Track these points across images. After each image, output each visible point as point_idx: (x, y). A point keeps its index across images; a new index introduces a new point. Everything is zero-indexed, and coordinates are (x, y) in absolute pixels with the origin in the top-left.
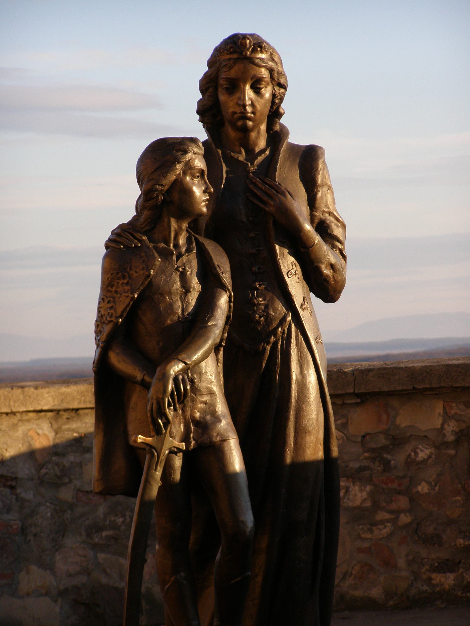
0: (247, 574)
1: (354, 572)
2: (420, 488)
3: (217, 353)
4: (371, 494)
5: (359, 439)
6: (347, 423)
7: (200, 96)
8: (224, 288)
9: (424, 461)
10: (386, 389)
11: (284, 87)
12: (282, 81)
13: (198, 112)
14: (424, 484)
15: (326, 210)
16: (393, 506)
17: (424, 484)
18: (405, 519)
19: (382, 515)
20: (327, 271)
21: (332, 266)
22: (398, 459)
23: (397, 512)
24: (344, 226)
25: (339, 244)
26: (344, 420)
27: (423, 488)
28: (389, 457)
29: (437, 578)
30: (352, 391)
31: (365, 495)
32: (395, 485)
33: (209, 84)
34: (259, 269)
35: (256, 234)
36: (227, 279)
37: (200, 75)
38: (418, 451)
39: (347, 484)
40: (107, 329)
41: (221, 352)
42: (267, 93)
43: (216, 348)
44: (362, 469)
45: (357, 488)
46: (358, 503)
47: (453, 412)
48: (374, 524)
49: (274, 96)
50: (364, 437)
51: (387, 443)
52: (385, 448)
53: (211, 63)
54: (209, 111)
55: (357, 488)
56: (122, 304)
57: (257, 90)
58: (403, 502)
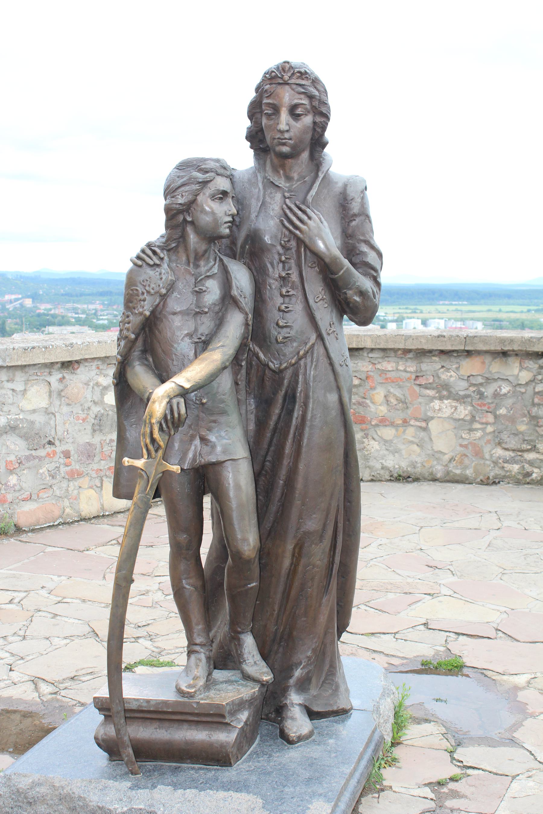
0: (252, 585)
1: (456, 459)
2: (501, 411)
3: (236, 374)
5: (466, 378)
9: (505, 395)
10: (484, 349)
11: (327, 117)
12: (324, 110)
13: (247, 138)
14: (504, 408)
15: (362, 238)
16: (484, 420)
17: (504, 408)
18: (490, 429)
19: (477, 426)
20: (357, 299)
21: (362, 293)
22: (489, 391)
23: (487, 424)
24: (380, 255)
26: (457, 365)
27: (502, 411)
29: (508, 466)
30: (462, 348)
31: (467, 412)
33: (255, 110)
35: (286, 258)
36: (247, 303)
38: (502, 388)
39: (457, 404)
40: (123, 343)
42: (308, 120)
45: (462, 407)
46: (462, 417)
47: (526, 366)
48: (471, 430)
50: (469, 377)
51: (484, 381)
52: (481, 384)
53: (257, 90)
55: (462, 407)
58: (490, 418)
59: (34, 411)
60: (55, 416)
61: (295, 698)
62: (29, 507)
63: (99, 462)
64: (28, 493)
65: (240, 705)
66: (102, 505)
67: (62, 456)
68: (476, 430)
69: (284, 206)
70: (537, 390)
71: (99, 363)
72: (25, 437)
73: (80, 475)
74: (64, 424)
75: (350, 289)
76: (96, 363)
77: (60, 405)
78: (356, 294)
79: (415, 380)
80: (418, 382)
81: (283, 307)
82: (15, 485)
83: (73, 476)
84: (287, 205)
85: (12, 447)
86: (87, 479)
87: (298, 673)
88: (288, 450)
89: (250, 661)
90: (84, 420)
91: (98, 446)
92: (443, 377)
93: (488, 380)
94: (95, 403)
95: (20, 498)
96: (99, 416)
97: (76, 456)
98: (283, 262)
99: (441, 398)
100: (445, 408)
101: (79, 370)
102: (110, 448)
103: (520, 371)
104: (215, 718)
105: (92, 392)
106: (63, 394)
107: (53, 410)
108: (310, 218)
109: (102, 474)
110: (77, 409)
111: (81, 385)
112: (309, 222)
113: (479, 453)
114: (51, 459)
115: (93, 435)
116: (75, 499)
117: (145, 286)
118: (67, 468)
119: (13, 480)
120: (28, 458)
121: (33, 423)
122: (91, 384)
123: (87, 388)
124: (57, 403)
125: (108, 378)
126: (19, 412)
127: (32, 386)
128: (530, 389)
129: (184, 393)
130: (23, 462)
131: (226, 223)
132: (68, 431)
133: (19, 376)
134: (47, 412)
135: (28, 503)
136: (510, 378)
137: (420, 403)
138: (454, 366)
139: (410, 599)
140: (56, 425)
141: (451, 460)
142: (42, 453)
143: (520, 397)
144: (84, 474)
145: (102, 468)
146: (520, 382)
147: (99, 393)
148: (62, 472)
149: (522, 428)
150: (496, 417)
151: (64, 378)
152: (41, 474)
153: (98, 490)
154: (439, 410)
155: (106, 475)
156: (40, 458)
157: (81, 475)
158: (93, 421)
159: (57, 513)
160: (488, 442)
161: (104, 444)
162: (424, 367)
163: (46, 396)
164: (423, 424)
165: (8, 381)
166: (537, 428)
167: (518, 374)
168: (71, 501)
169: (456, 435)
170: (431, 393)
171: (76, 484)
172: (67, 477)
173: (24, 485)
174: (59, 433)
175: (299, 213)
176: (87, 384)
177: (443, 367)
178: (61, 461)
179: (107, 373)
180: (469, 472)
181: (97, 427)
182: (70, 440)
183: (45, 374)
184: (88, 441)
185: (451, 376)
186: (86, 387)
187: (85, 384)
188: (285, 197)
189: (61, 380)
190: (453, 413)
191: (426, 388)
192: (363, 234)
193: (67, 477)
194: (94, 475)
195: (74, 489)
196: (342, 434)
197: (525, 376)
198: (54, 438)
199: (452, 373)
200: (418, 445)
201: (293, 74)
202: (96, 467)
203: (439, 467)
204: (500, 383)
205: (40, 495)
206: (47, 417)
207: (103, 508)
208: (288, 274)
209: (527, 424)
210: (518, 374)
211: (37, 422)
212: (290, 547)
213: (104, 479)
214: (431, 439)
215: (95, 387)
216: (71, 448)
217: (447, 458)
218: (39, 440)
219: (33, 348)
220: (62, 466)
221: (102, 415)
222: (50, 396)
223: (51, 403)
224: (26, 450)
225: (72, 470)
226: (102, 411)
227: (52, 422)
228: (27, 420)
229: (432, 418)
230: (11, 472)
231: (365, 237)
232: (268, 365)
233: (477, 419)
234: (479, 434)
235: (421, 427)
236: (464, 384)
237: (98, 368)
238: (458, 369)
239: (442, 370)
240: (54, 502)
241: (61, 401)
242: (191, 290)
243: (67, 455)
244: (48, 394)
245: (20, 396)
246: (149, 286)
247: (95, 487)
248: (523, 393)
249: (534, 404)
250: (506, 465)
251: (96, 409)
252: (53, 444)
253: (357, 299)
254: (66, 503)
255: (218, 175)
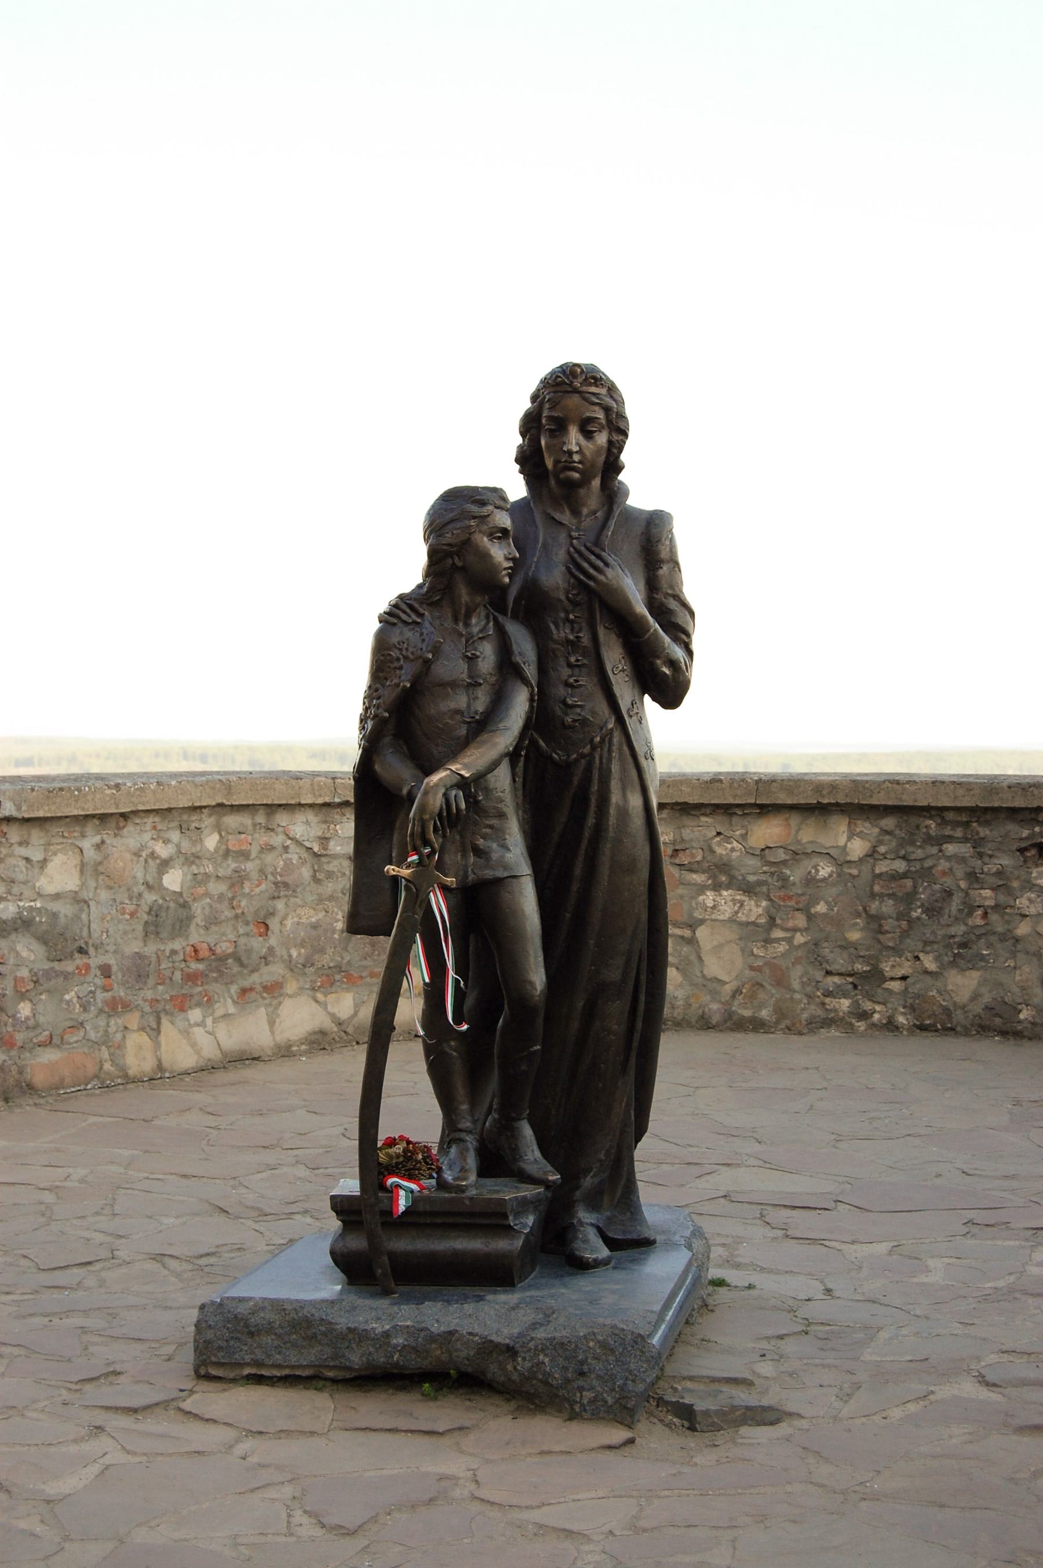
0: (535, 1048)
1: (744, 991)
3: (513, 766)
4: (767, 910)
5: (758, 852)
6: (746, 834)
7: (519, 440)
8: (526, 681)
9: (824, 880)
10: (789, 802)
11: (625, 434)
12: (622, 426)
13: (517, 461)
14: (822, 903)
15: (670, 592)
16: (790, 924)
17: (822, 903)
18: (799, 939)
19: (777, 934)
20: (666, 670)
21: (673, 664)
22: (795, 875)
23: (795, 930)
25: (684, 637)
26: (744, 831)
27: (821, 908)
28: (788, 872)
30: (753, 801)
31: (760, 911)
32: (792, 903)
33: (530, 424)
34: (577, 660)
36: (531, 671)
37: (521, 414)
38: (819, 868)
39: (743, 898)
40: (370, 725)
41: (521, 764)
43: (513, 756)
44: (760, 883)
45: (753, 902)
47: (858, 830)
48: (768, 941)
49: (610, 442)
51: (788, 858)
52: (784, 863)
53: (534, 398)
54: (529, 460)
55: (753, 902)
56: (389, 695)
57: (588, 435)
58: (801, 921)
59: (57, 896)
60: (89, 906)
61: (585, 1216)
62: (49, 1056)
63: (154, 987)
64: (47, 1033)
65: (524, 1205)
66: (159, 1060)
67: (99, 973)
68: (778, 940)
69: (572, 549)
70: (877, 871)
71: (157, 819)
72: (43, 939)
73: (127, 1007)
74: (103, 919)
75: (658, 657)
76: (150, 820)
77: (96, 888)
78: (665, 663)
79: (672, 856)
80: (677, 861)
81: (571, 680)
82: (27, 1018)
83: (115, 1007)
84: (574, 548)
85: (25, 954)
86: (137, 1014)
87: (588, 1182)
88: (578, 870)
89: (530, 1157)
90: (132, 914)
91: (154, 959)
92: (719, 850)
93: (797, 855)
94: (149, 887)
95: (35, 1040)
96: (155, 909)
97: (120, 975)
98: (572, 622)
99: (717, 887)
100: (723, 903)
101: (125, 830)
102: (170, 965)
103: (849, 839)
104: (492, 1219)
105: (145, 868)
106: (101, 869)
107: (84, 895)
108: (607, 564)
109: (160, 1007)
110: (122, 896)
111: (128, 856)
112: (606, 569)
113: (781, 981)
114: (82, 978)
115: (145, 941)
116: (118, 1048)
117: (400, 650)
118: (105, 994)
119: (25, 1009)
120: (49, 974)
121: (55, 915)
122: (144, 854)
123: (138, 862)
124: (92, 884)
125: (169, 846)
126: (36, 896)
127: (55, 854)
128: (866, 868)
129: (463, 784)
130: (41, 981)
131: (506, 569)
132: (107, 932)
133: (37, 836)
134: (78, 899)
135: (48, 1050)
136: (832, 852)
137: (681, 897)
138: (738, 833)
139: (696, 1170)
140: (90, 921)
141: (737, 992)
142: (69, 966)
143: (849, 884)
144: (132, 1006)
145: (159, 998)
146: (848, 858)
147: (155, 870)
148: (99, 1001)
149: (855, 936)
150: (810, 917)
151: (103, 842)
152: (68, 1002)
153: (153, 1034)
154: (714, 907)
155: (165, 1010)
156: (66, 976)
157: (128, 1006)
158: (145, 917)
159: (91, 1069)
160: (798, 961)
161: (162, 957)
162: (687, 834)
163: (76, 874)
164: (687, 933)
165: (20, 844)
166: (880, 936)
167: (846, 845)
168: (112, 1050)
169: (743, 951)
170: (698, 878)
171: (120, 1021)
172: (106, 1009)
173: (41, 1019)
174: (95, 935)
175: (593, 558)
176: (137, 854)
177: (719, 834)
178: (99, 981)
179: (167, 836)
180: (764, 1014)
181: (152, 928)
182: (111, 948)
183: (76, 834)
184: (137, 950)
185: (733, 850)
186: (135, 858)
187: (135, 854)
188: (571, 537)
189: (98, 847)
190: (737, 913)
191: (691, 871)
192: (672, 587)
193: (106, 1009)
194: (147, 1009)
195: (117, 1031)
196: (647, 850)
197: (857, 848)
198: (86, 943)
199: (735, 844)
200: (677, 968)
201: (586, 379)
202: (149, 994)
203: (715, 1006)
204: (815, 860)
205: (66, 1037)
206: (77, 907)
207: (160, 1067)
208: (577, 637)
209: (861, 930)
210: (846, 845)
211: (61, 916)
212: (580, 1004)
213: (162, 1015)
214: (700, 958)
215: (150, 860)
216: (111, 960)
217: (728, 989)
218: (64, 943)
219: (61, 789)
220: (98, 991)
221: (161, 907)
222: (82, 872)
223: (83, 884)
224: (45, 960)
225: (114, 998)
226: (161, 901)
227: (84, 916)
228: (46, 910)
229: (702, 922)
230: (22, 996)
231: (674, 590)
232: (551, 758)
233: (778, 921)
234: (782, 948)
235: (682, 937)
236: (753, 862)
237: (154, 828)
238: (744, 836)
239: (718, 839)
240: (86, 1050)
241: (97, 881)
242: (460, 655)
243: (106, 971)
244: (78, 868)
245: (36, 871)
246: (407, 649)
247: (148, 1029)
248: (854, 877)
249: (873, 895)
250: (827, 1000)
251: (150, 898)
252: (86, 953)
253: (666, 670)
254: (105, 1054)
255: (497, 508)
